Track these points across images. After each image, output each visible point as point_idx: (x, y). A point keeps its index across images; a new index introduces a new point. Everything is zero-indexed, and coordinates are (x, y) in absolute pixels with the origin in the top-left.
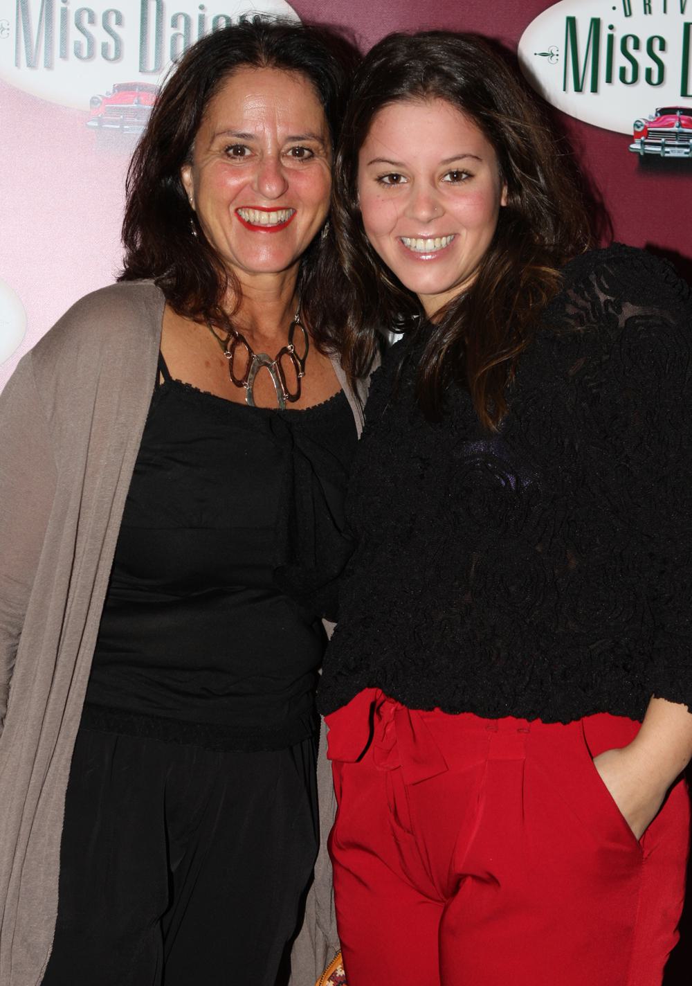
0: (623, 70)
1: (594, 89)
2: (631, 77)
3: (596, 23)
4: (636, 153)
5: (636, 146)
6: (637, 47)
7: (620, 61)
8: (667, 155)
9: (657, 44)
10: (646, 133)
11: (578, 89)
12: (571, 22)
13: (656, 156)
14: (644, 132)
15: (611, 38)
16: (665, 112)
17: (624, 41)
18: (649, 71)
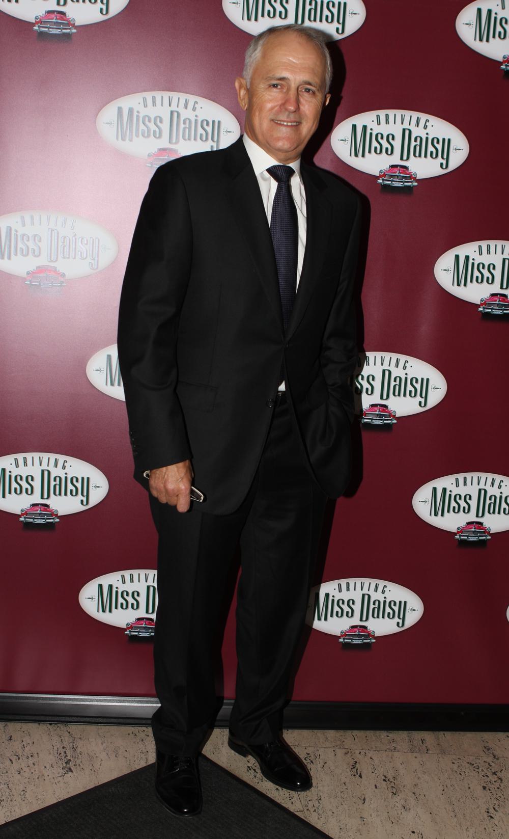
3: (490, 11)
7: (499, 29)
12: (479, 10)
15: (496, 18)
17: (501, 20)
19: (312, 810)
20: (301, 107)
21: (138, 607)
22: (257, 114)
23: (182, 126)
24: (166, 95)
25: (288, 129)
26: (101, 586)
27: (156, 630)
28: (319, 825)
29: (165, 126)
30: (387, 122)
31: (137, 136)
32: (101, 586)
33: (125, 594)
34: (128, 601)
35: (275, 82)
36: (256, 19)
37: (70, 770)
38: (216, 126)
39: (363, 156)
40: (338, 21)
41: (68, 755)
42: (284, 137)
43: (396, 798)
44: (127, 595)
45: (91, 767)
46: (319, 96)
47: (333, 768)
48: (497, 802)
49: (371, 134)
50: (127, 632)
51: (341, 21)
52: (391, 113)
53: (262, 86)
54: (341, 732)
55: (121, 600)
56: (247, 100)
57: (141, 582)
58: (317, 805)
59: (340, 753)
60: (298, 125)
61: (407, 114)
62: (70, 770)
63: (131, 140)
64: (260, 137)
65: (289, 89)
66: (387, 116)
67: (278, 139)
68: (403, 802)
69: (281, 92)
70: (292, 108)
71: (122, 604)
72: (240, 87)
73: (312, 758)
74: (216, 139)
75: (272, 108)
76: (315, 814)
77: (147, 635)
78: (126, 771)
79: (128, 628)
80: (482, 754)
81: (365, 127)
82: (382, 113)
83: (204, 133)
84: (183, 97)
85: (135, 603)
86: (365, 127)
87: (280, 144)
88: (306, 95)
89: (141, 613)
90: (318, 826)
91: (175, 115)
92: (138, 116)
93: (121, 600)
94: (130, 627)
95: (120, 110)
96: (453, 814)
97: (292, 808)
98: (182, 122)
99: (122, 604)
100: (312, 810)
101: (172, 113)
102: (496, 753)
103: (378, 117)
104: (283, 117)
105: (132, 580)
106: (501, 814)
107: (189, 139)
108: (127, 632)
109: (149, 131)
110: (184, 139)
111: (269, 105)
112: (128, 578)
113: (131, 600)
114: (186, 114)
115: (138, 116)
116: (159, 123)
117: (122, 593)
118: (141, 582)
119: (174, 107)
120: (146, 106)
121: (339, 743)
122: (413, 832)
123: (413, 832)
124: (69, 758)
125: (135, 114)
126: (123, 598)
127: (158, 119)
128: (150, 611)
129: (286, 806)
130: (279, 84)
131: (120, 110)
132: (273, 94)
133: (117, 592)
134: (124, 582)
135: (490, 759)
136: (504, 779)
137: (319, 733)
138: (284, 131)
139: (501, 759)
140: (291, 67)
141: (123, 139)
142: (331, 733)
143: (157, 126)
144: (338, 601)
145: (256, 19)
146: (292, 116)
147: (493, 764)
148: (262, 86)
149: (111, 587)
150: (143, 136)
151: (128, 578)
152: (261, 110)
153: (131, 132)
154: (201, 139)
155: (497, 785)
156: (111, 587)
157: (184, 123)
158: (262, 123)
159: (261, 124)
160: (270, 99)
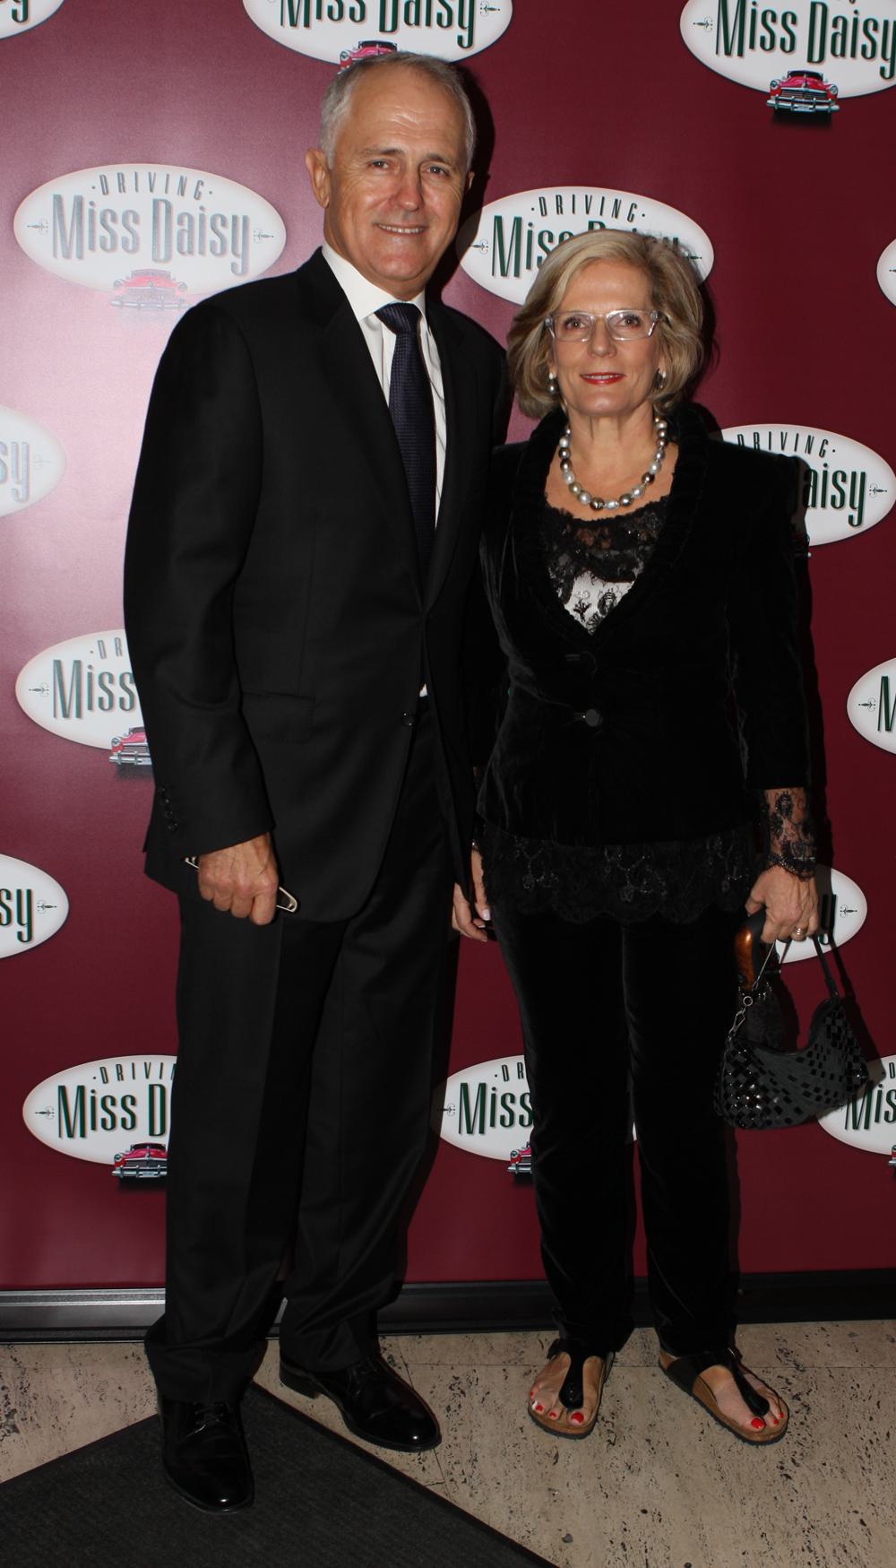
0: (763, 39)
1: (741, 54)
2: (769, 45)
4: (772, 107)
5: (771, 102)
6: (774, 20)
9: (789, 18)
10: (780, 91)
11: (728, 53)
13: (787, 110)
14: (778, 90)
15: (754, 12)
16: (794, 74)
18: (783, 41)
19: (459, 1481)
20: (427, 201)
21: (134, 1125)
22: (349, 214)
23: (176, 228)
24: (144, 170)
25: (407, 241)
26: (62, 1090)
27: (170, 1164)
28: (471, 1508)
29: (144, 229)
30: (560, 210)
31: (92, 248)
32: (62, 1090)
33: (109, 1101)
34: (115, 1114)
35: (377, 158)
36: (307, 24)
37: (15, 1429)
38: (241, 225)
40: (461, 25)
41: (12, 1399)
42: (398, 252)
43: (615, 1451)
44: (113, 1103)
45: (53, 1421)
46: (457, 180)
47: (500, 1402)
48: (799, 1450)
49: (530, 233)
50: (117, 1172)
51: (466, 24)
52: (566, 192)
53: (355, 166)
54: (519, 1335)
55: (101, 1114)
56: (327, 189)
57: (143, 1078)
58: (469, 1470)
59: (515, 1373)
60: (423, 229)
61: (597, 193)
62: (15, 1429)
63: (80, 257)
64: (356, 254)
65: (403, 171)
66: (559, 199)
67: (389, 259)
68: (627, 1457)
69: (391, 174)
70: (411, 204)
71: (104, 1121)
72: (315, 167)
73: (464, 1385)
74: (240, 251)
75: (375, 205)
76: (465, 1487)
77: (153, 1175)
78: (118, 1426)
79: (117, 1164)
80: (776, 1363)
81: (518, 221)
82: (550, 194)
83: (218, 240)
84: (176, 173)
85: (128, 1117)
86: (518, 221)
87: (392, 267)
88: (433, 177)
89: (141, 1135)
90: (471, 1510)
91: (163, 207)
92: (92, 213)
93: (101, 1114)
94: (122, 1162)
95: (58, 200)
96: (717, 1475)
97: (422, 1479)
98: (175, 220)
99: (104, 1121)
100: (459, 1481)
101: (156, 203)
102: (800, 1360)
103: (542, 201)
104: (396, 219)
105: (120, 1076)
106: (806, 1471)
107: (191, 252)
108: (117, 1172)
109: (114, 237)
110: (181, 252)
111: (369, 199)
112: (112, 1073)
113: (119, 1113)
114: (183, 205)
115: (92, 213)
116: (131, 224)
117: (104, 1100)
118: (143, 1078)
119: (159, 193)
120: (106, 192)
121: (513, 1355)
122: (644, 1512)
123: (644, 1512)
124: (12, 1406)
125: (87, 207)
126: (108, 1108)
127: (131, 217)
128: (158, 1130)
129: (413, 1476)
130: (387, 160)
131: (58, 200)
132: (376, 179)
133: (93, 1099)
134: (105, 1080)
135: (788, 1372)
136: (813, 1407)
137: (478, 1339)
138: (396, 245)
139: (810, 1372)
140: (407, 132)
141: (67, 256)
142: (500, 1339)
143: (128, 229)
144: (504, 1098)
145: (307, 24)
146: (412, 217)
147: (794, 1381)
148: (355, 165)
149: (81, 1089)
150: (103, 247)
151: (112, 1073)
152: (355, 207)
153: (80, 240)
154: (213, 251)
155: (800, 1417)
156: (81, 1089)
157: (180, 222)
158: (358, 230)
159: (356, 232)
160: (371, 188)
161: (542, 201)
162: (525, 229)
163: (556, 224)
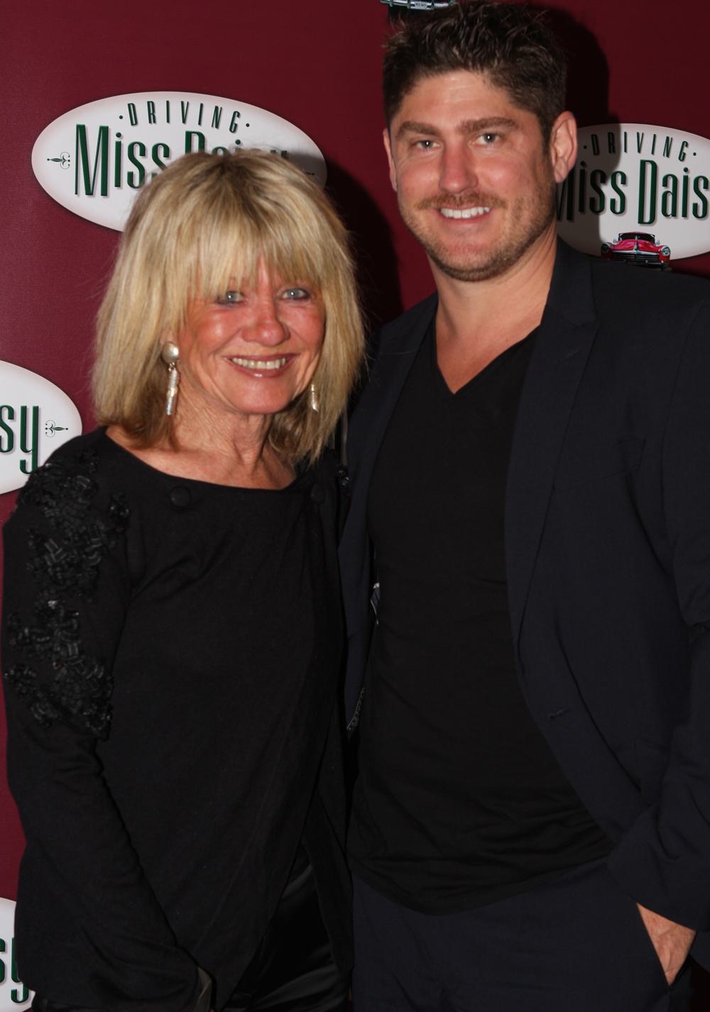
8: (412, 7)
30: (152, 118)
39: (105, 192)
49: (119, 145)
52: (159, 98)
61: (194, 100)
66: (151, 106)
81: (104, 131)
82: (140, 100)
86: (104, 131)
103: (132, 108)
161: (132, 108)
162: (113, 140)
163: (147, 134)
